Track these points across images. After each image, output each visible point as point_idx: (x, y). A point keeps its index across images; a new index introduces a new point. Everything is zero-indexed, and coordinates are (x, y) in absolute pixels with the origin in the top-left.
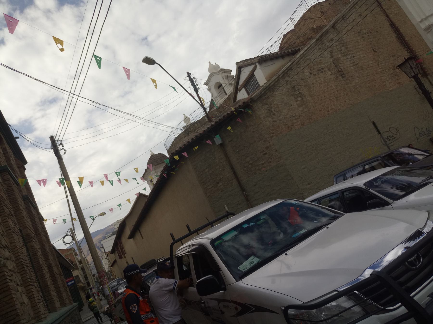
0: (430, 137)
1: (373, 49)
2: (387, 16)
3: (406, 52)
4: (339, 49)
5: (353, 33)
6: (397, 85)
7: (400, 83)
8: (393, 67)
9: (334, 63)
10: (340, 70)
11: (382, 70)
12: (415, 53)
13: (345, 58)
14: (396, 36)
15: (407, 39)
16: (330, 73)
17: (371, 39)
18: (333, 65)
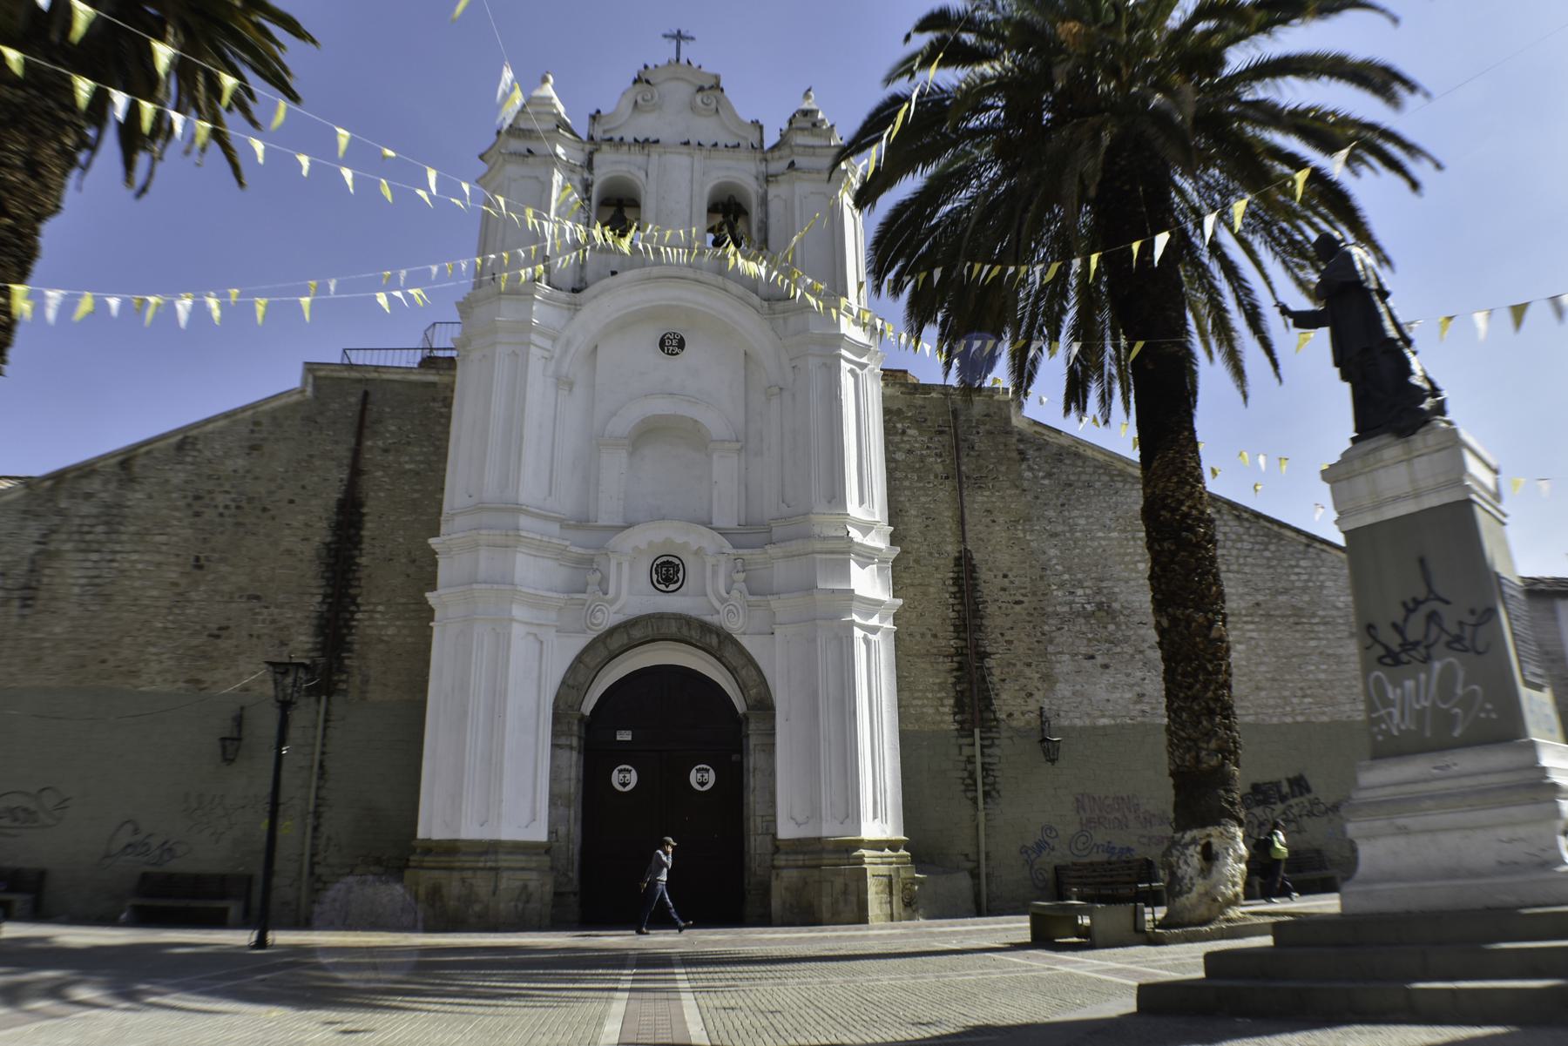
0: (148, 869)
1: (197, 559)
2: (356, 471)
3: (319, 598)
4: (86, 529)
6: (181, 684)
7: (198, 681)
8: (220, 629)
9: (33, 562)
11: (170, 625)
12: (353, 613)
13: (81, 556)
14: (328, 539)
15: (363, 560)
17: (222, 525)
18: (25, 567)
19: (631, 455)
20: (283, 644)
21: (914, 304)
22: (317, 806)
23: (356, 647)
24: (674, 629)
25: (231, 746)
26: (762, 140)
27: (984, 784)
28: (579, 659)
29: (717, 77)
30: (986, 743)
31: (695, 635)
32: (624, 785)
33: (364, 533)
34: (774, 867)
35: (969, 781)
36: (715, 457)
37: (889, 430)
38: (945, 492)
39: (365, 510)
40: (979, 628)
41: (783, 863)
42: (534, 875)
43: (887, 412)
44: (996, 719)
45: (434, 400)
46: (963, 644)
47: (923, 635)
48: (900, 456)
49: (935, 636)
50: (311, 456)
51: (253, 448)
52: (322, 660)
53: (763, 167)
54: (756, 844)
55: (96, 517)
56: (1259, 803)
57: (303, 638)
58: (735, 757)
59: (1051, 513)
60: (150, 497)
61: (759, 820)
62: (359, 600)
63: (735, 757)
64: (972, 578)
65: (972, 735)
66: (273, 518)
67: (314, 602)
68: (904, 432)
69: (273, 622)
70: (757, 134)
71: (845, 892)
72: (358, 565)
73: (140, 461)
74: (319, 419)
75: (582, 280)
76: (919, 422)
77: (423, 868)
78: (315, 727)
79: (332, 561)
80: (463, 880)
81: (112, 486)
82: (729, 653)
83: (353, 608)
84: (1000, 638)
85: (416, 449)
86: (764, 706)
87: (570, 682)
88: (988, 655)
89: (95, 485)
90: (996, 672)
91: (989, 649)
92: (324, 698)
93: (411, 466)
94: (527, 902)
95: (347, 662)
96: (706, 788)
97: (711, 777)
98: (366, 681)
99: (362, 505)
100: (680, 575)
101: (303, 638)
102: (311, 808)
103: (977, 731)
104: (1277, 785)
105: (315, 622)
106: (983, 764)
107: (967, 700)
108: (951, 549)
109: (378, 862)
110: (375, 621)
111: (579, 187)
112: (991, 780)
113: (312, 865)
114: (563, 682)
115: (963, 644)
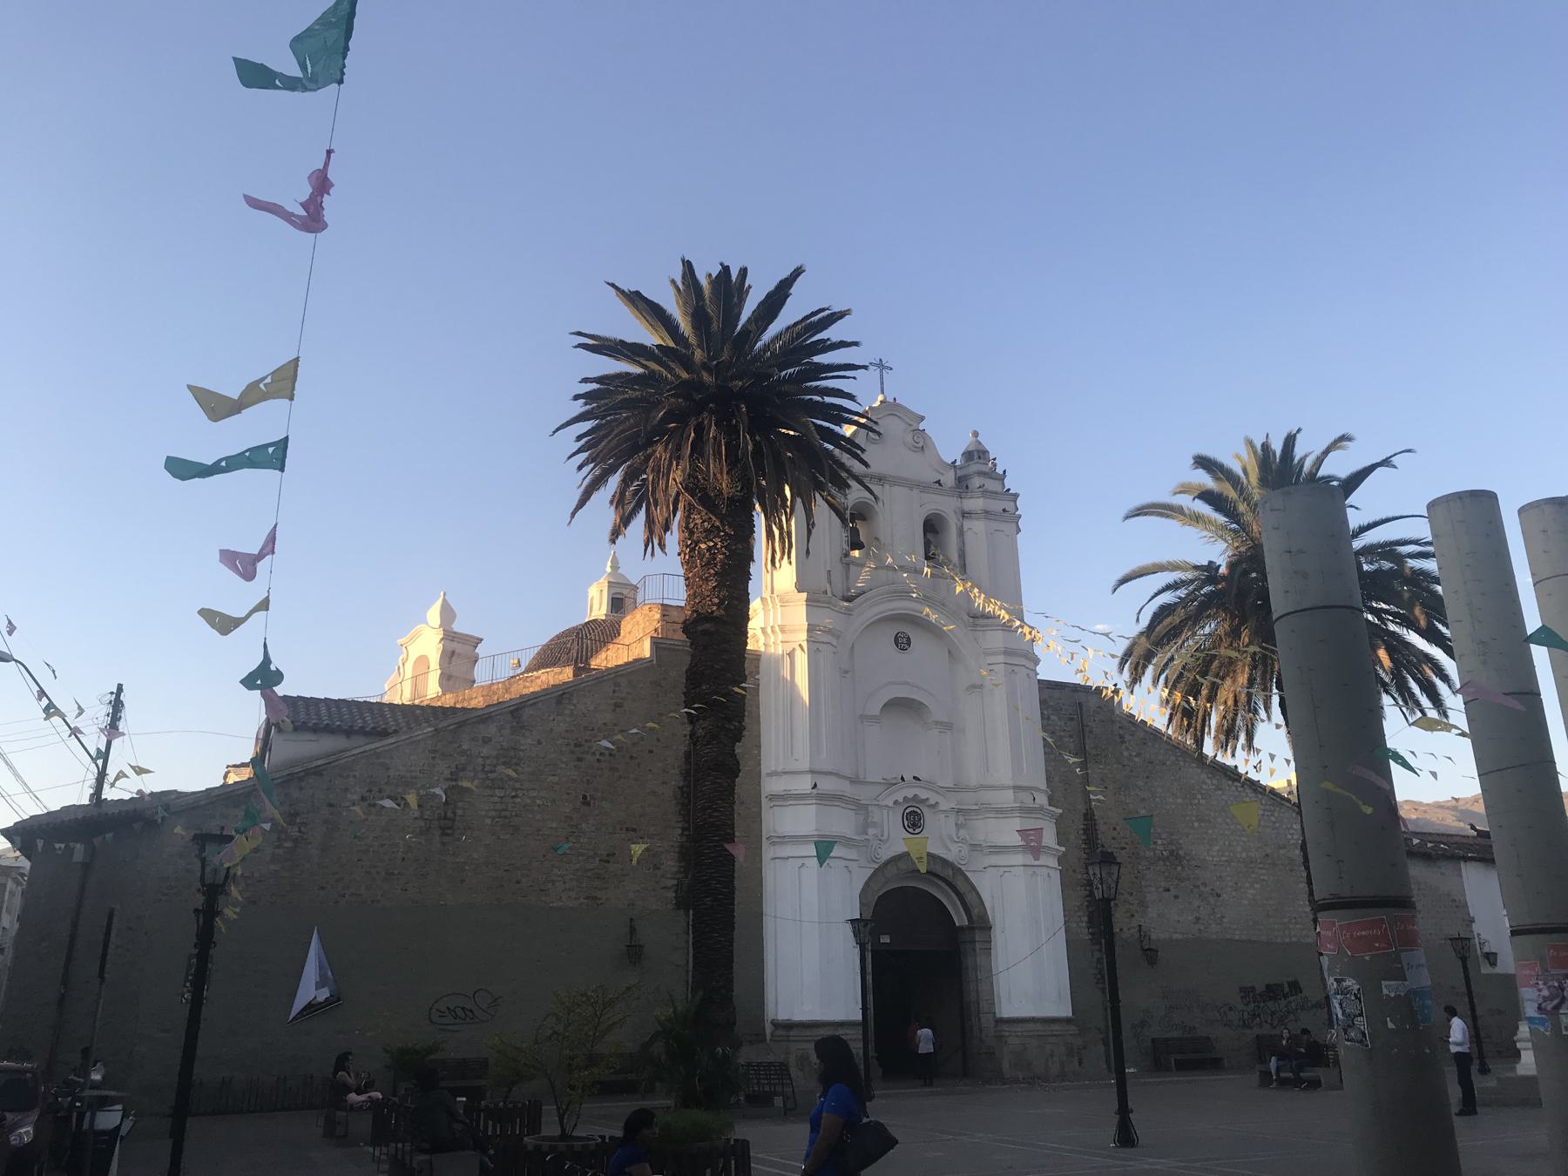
1: (585, 797)
5: (560, 742)
10: (449, 814)
13: (488, 792)
16: (417, 814)
20: (657, 868)
25: (634, 953)
28: (867, 884)
29: (923, 418)
51: (617, 705)
55: (497, 757)
56: (1271, 999)
59: (1140, 783)
60: (539, 742)
73: (527, 713)
81: (506, 732)
82: (960, 884)
86: (981, 925)
89: (491, 729)
104: (1281, 986)
108: (1082, 808)
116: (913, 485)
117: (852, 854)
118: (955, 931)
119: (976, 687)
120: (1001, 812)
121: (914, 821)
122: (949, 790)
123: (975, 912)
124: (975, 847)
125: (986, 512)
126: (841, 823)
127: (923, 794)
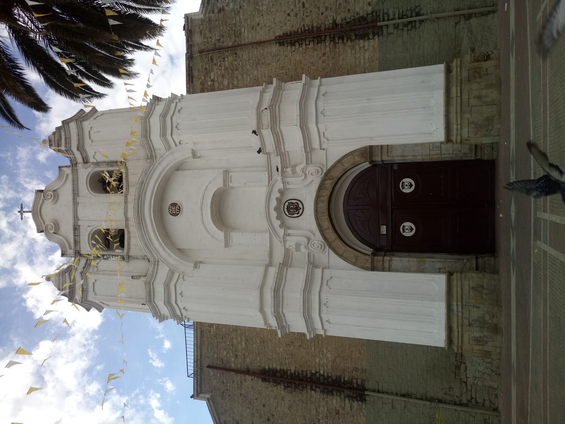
2: (248, 372)
3: (313, 392)
12: (320, 375)
14: (283, 387)
15: (293, 369)
19: (234, 229)
20: (338, 413)
21: (118, 74)
22: (427, 400)
23: (338, 374)
24: (324, 206)
26: (66, 167)
27: (412, 16)
28: (341, 256)
30: (386, 18)
31: (326, 193)
32: (412, 229)
33: (279, 369)
34: (461, 142)
35: (409, 27)
36: (231, 185)
37: (212, 89)
38: (244, 55)
39: (267, 368)
40: (318, 28)
41: (459, 137)
42: (466, 283)
43: (202, 91)
44: (372, 13)
45: (210, 332)
46: (328, 39)
47: (324, 62)
48: (225, 82)
49: (324, 54)
50: (241, 394)
52: (347, 392)
53: (80, 166)
54: (448, 153)
57: (334, 402)
58: (395, 167)
61: (432, 153)
62: (314, 372)
63: (395, 167)
64: (290, 35)
65: (381, 27)
66: (273, 415)
67: (316, 395)
68: (213, 81)
69: (327, 417)
70: (64, 169)
71: (480, 97)
72: (295, 371)
74: (221, 391)
75: (144, 259)
76: (207, 72)
77: (462, 346)
78: (382, 398)
79: (293, 385)
80: (470, 325)
82: (337, 173)
83: (318, 375)
84: (324, 14)
85: (235, 341)
87: (353, 260)
88: (334, 22)
90: (343, 15)
91: (331, 21)
92: (366, 393)
93: (243, 343)
94: (483, 287)
95: (346, 379)
96: (413, 183)
97: (407, 181)
98: (356, 369)
99: (264, 369)
100: (294, 201)
101: (334, 402)
102: (428, 403)
103: (379, 24)
105: (325, 396)
106: (399, 19)
107: (361, 33)
108: (275, 48)
109: (458, 367)
110: (324, 364)
111: (98, 261)
112: (409, 13)
113: (461, 405)
114: (354, 264)
115: (328, 39)
116: (75, 204)
117: (318, 272)
118: (374, 165)
119: (194, 155)
120: (279, 140)
121: (294, 208)
122: (270, 177)
123: (357, 159)
124: (308, 161)
125: (78, 149)
126: (296, 278)
127: (274, 203)
